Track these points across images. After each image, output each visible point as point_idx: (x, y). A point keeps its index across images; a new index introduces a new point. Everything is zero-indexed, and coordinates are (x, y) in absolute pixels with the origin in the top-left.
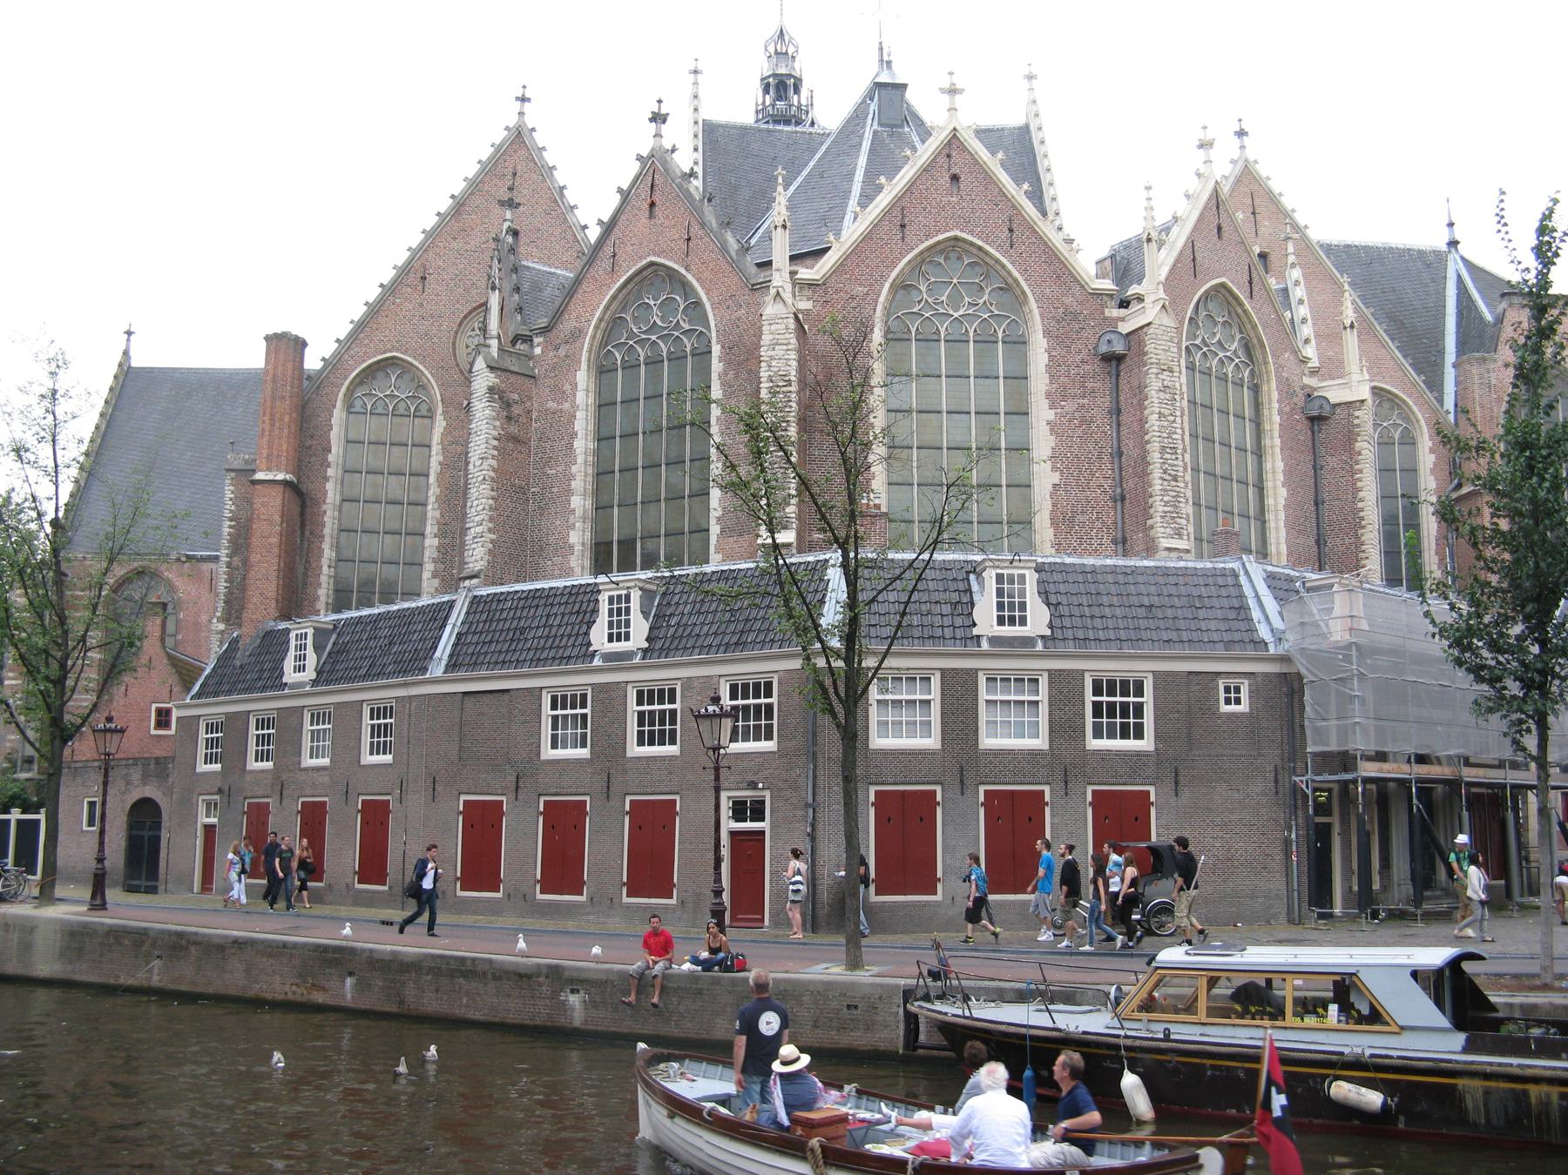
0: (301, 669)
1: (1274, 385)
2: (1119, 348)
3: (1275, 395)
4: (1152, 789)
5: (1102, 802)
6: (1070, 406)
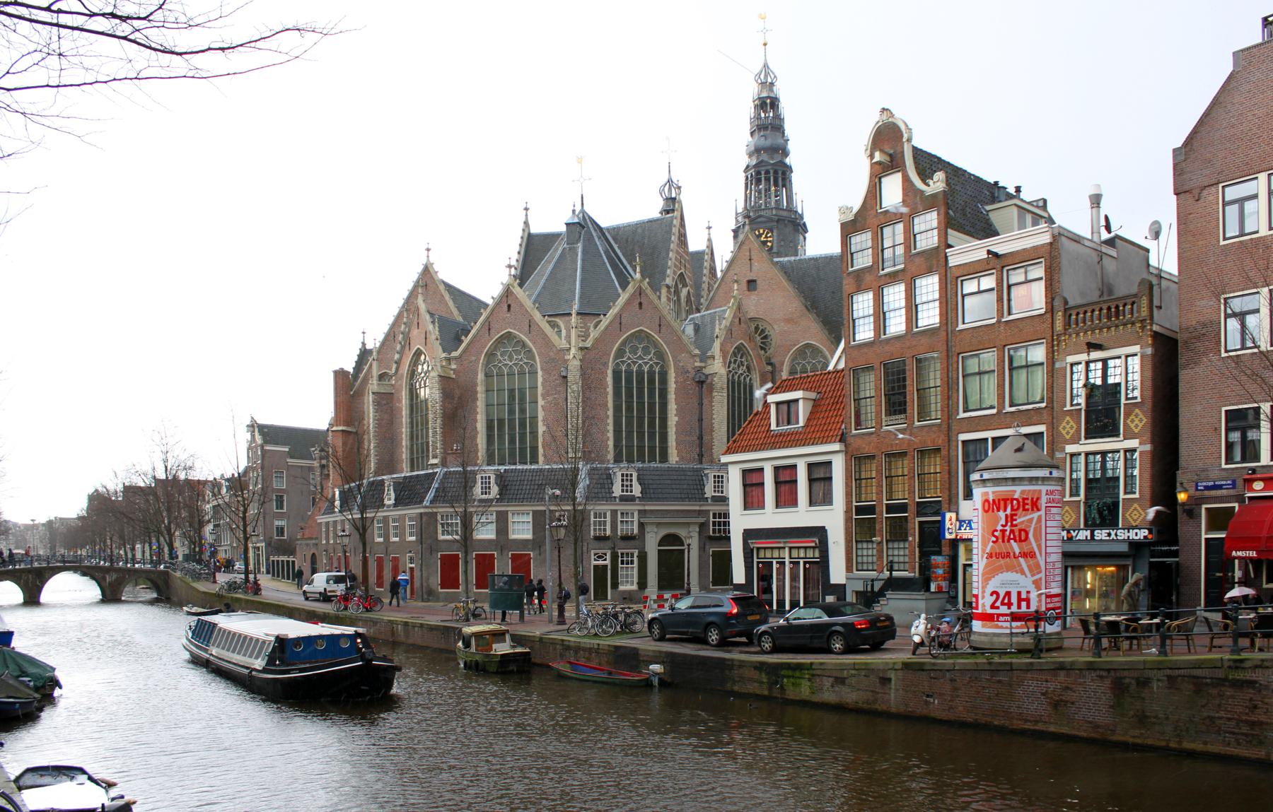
0: (389, 499)
1: (673, 370)
2: (564, 374)
3: (673, 375)
4: (532, 553)
5: (514, 557)
6: (550, 399)
